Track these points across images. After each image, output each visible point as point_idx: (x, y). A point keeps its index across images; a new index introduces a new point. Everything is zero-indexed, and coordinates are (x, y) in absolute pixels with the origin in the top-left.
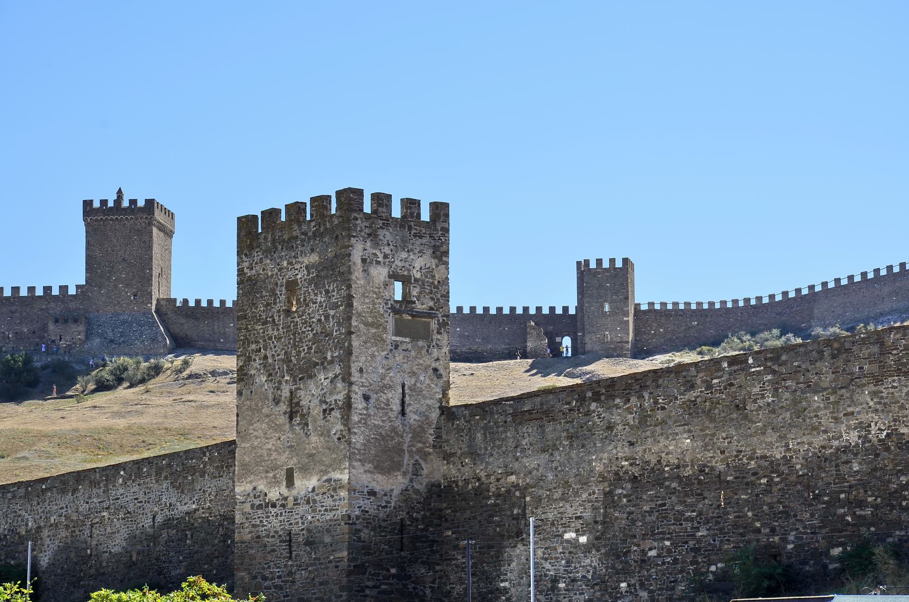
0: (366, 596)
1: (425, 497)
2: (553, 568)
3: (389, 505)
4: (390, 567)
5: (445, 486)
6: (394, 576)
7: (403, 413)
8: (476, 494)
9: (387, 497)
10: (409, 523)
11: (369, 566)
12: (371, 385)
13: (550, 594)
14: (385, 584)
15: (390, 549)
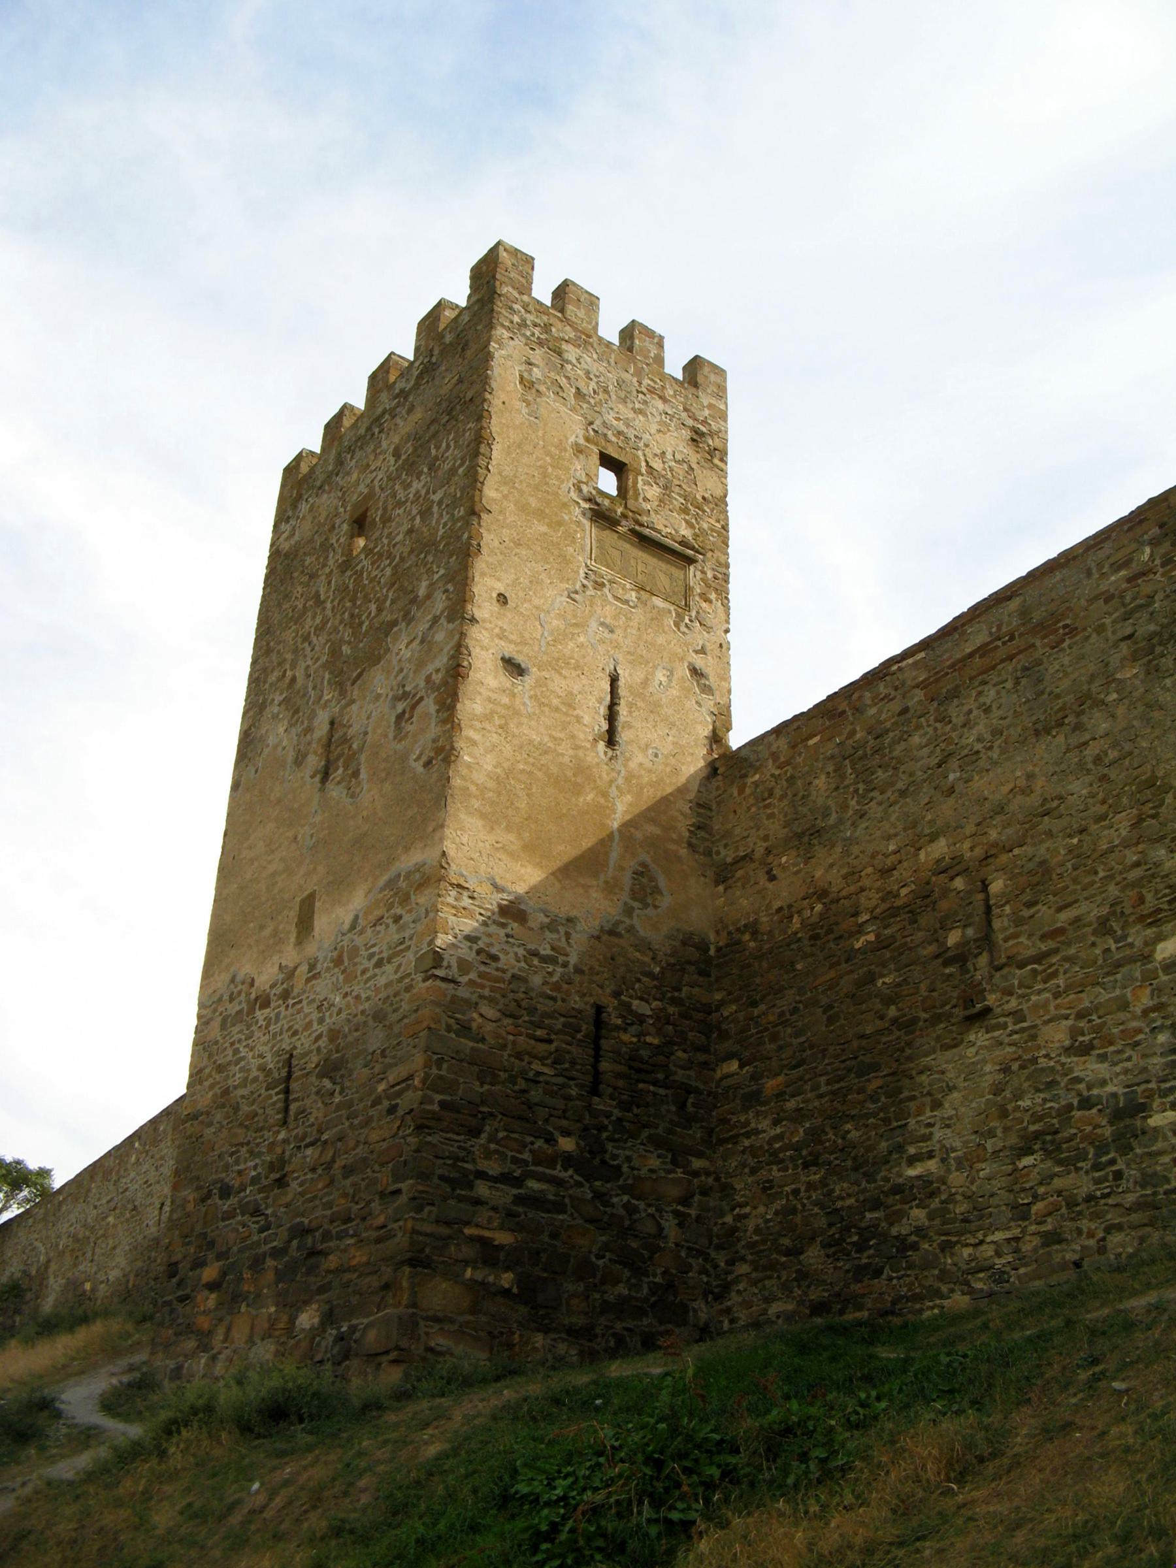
0: (478, 1202)
1: (664, 964)
2: (1118, 1069)
3: (561, 959)
4: (557, 1134)
5: (719, 949)
6: (568, 1160)
7: (611, 739)
8: (815, 937)
9: (555, 936)
10: (619, 1021)
11: (491, 1114)
12: (524, 643)
13: (1112, 1162)
14: (540, 1178)
15: (560, 1080)
